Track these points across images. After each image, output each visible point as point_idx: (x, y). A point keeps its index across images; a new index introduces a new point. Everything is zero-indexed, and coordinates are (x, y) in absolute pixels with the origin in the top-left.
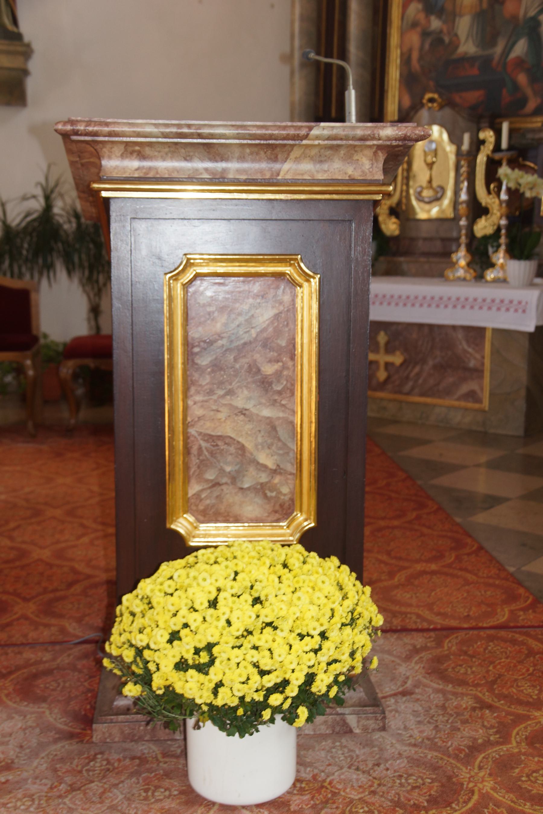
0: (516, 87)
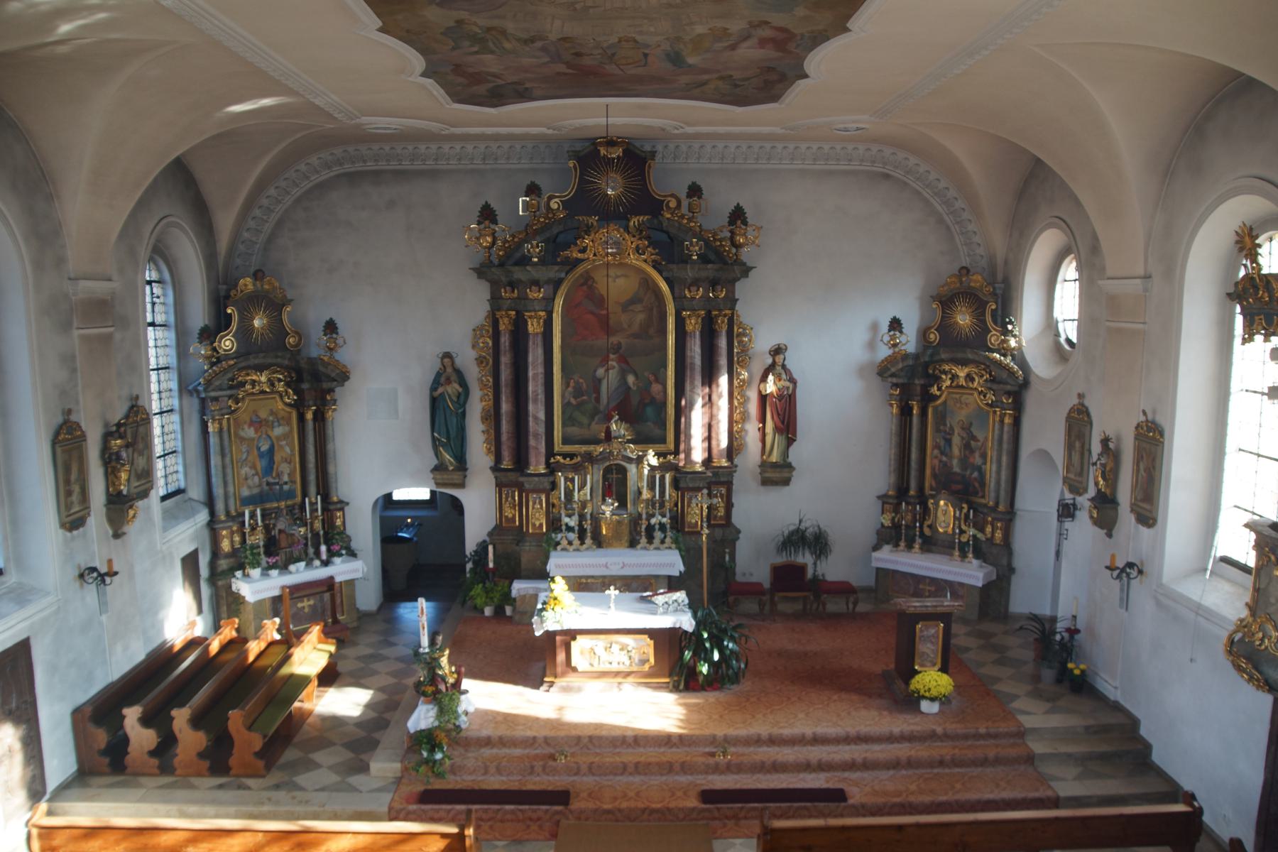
0: (974, 486)
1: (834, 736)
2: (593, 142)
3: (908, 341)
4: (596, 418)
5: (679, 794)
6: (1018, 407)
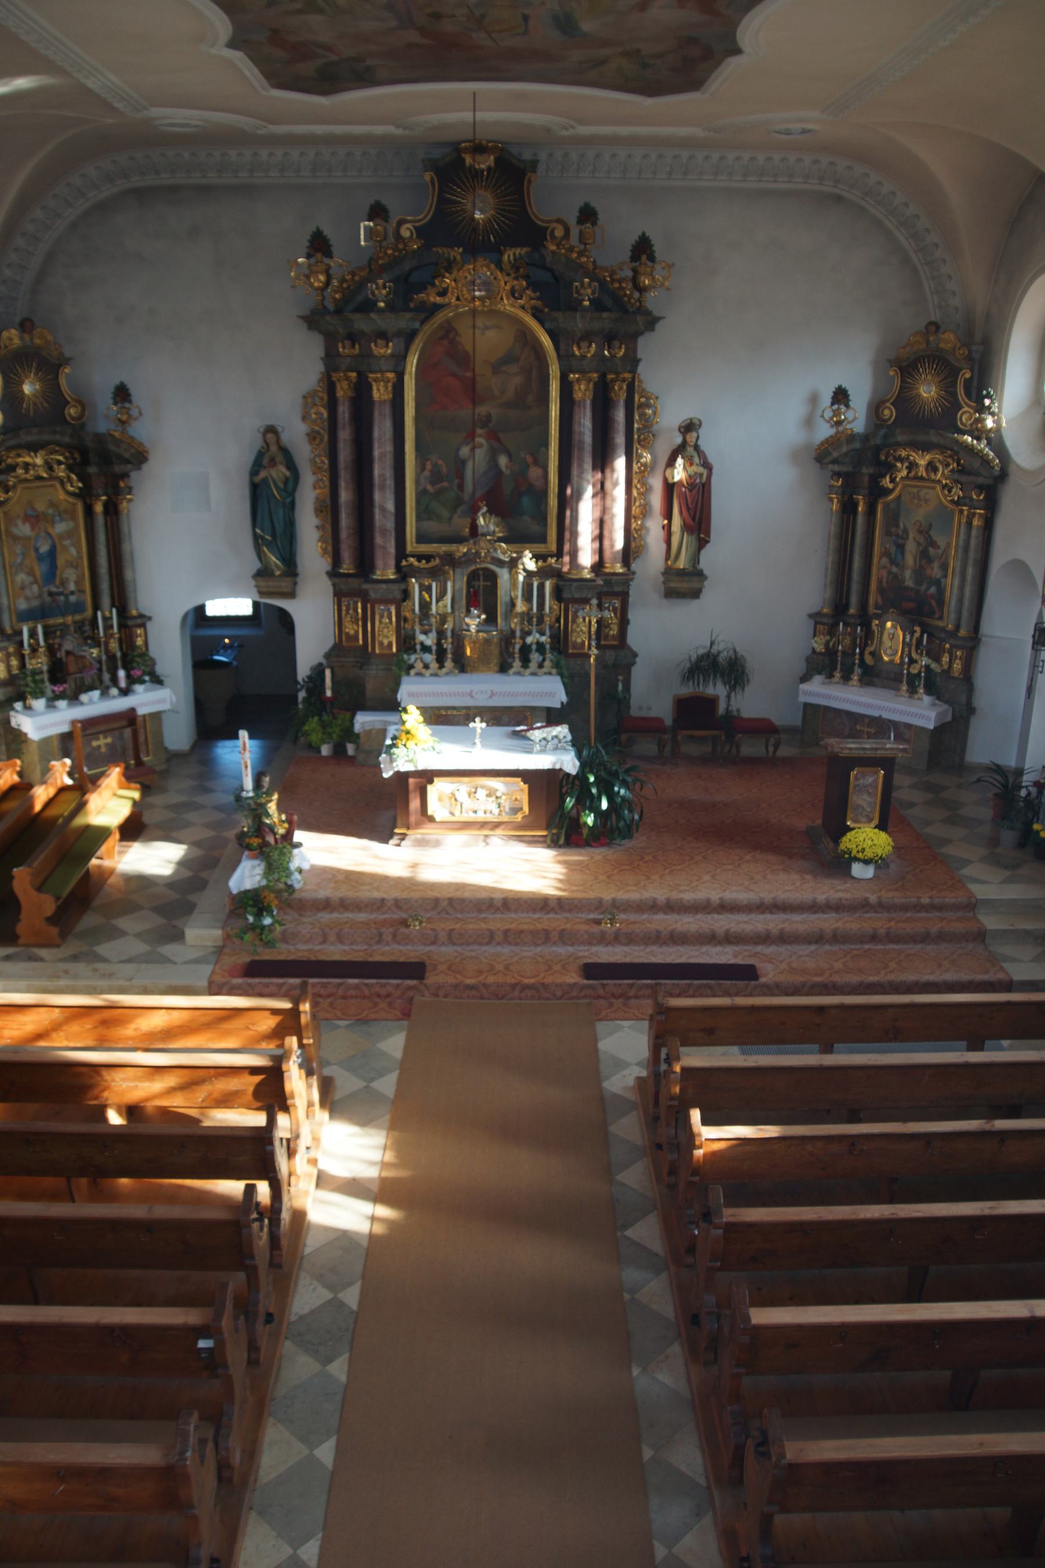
1: (745, 902)
2: (456, 147)
3: (855, 419)
4: (459, 510)
5: (557, 967)
6: (991, 505)
